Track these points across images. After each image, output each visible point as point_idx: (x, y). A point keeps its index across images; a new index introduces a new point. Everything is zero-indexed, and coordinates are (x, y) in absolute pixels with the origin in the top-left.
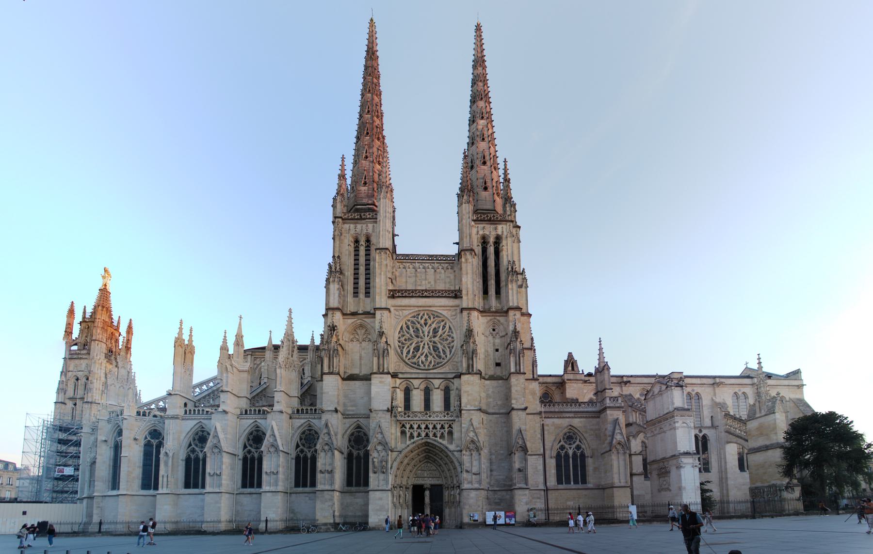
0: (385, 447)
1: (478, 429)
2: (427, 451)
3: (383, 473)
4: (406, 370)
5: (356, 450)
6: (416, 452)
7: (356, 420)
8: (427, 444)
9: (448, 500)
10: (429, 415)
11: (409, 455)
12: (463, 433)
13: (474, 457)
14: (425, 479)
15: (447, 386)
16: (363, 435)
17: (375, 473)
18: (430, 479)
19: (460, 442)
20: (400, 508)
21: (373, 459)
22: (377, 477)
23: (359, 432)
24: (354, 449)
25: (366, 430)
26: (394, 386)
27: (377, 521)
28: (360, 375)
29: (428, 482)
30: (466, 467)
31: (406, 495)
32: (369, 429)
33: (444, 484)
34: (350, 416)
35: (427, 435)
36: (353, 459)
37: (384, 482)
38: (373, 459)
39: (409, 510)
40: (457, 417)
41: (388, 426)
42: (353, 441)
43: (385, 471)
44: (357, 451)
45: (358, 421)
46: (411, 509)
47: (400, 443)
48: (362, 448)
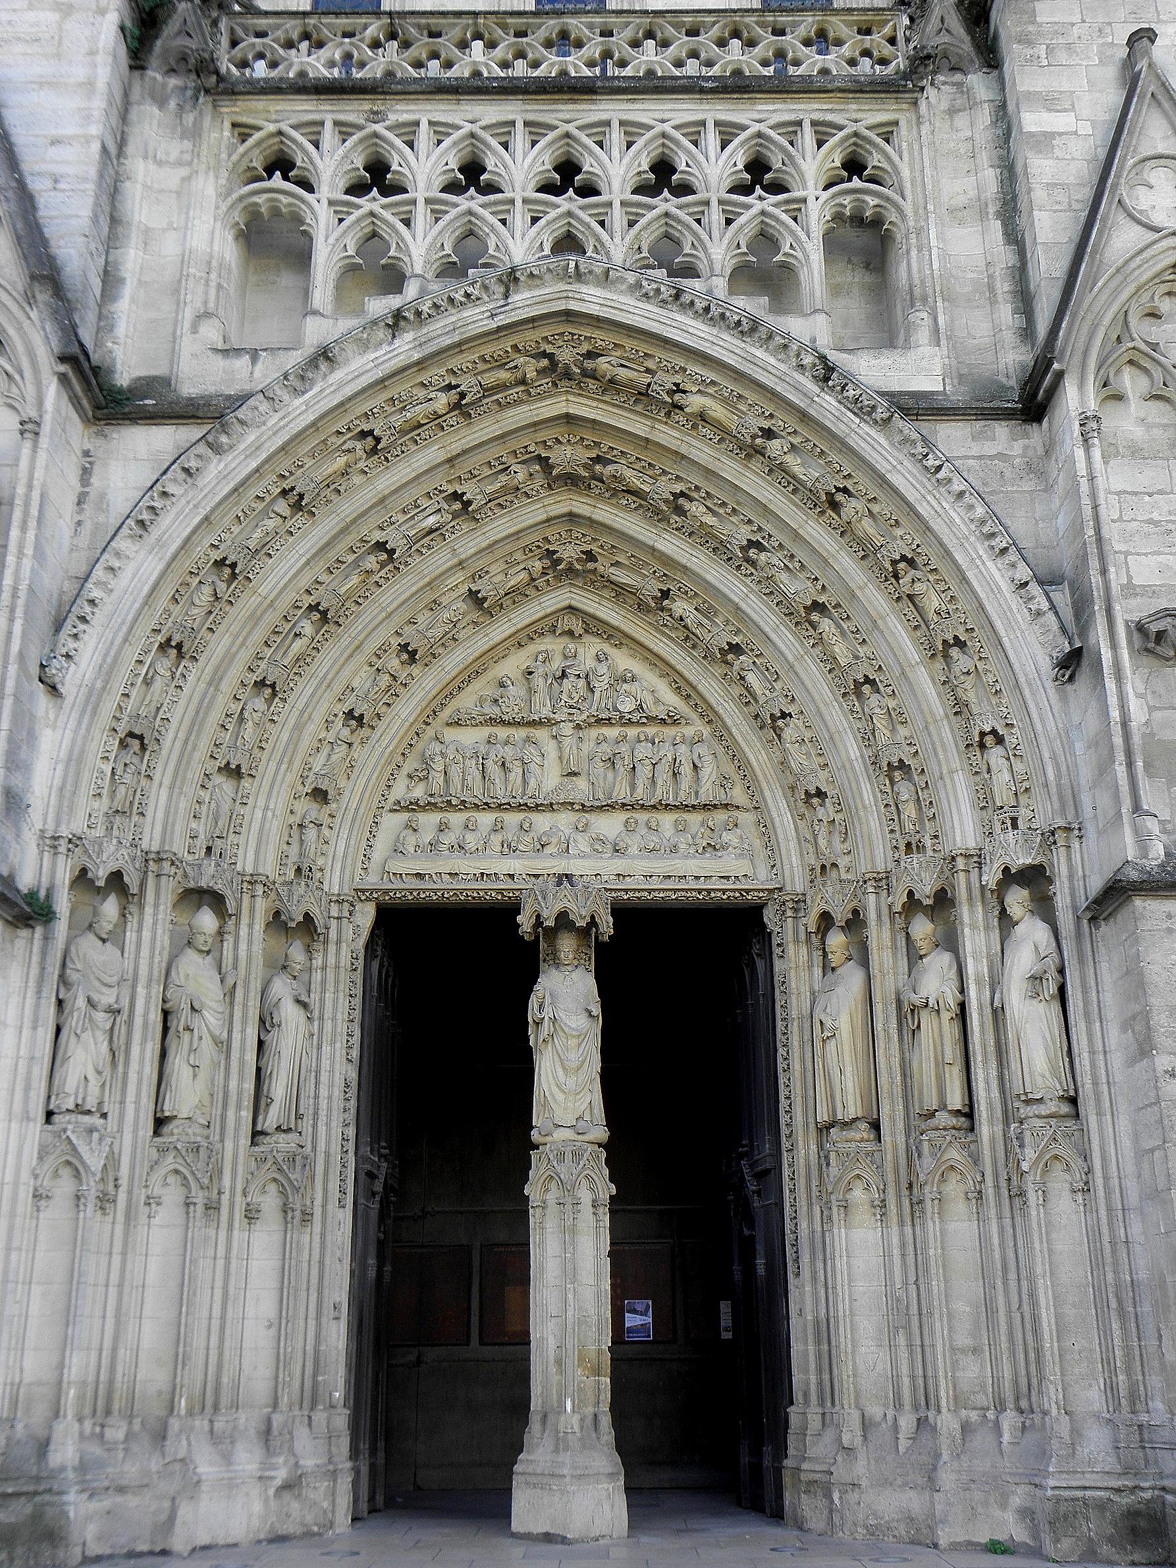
2: (567, 456)
6: (431, 454)
8: (566, 356)
9: (872, 1093)
10: (593, 49)
11: (335, 485)
14: (542, 822)
18: (610, 825)
19: (1006, 314)
20: (172, 1195)
29: (576, 867)
30: (1130, 589)
31: (266, 1022)
33: (796, 880)
35: (568, 243)
39: (309, 1239)
41: (70, 130)
46: (345, 1217)
47: (211, 333)
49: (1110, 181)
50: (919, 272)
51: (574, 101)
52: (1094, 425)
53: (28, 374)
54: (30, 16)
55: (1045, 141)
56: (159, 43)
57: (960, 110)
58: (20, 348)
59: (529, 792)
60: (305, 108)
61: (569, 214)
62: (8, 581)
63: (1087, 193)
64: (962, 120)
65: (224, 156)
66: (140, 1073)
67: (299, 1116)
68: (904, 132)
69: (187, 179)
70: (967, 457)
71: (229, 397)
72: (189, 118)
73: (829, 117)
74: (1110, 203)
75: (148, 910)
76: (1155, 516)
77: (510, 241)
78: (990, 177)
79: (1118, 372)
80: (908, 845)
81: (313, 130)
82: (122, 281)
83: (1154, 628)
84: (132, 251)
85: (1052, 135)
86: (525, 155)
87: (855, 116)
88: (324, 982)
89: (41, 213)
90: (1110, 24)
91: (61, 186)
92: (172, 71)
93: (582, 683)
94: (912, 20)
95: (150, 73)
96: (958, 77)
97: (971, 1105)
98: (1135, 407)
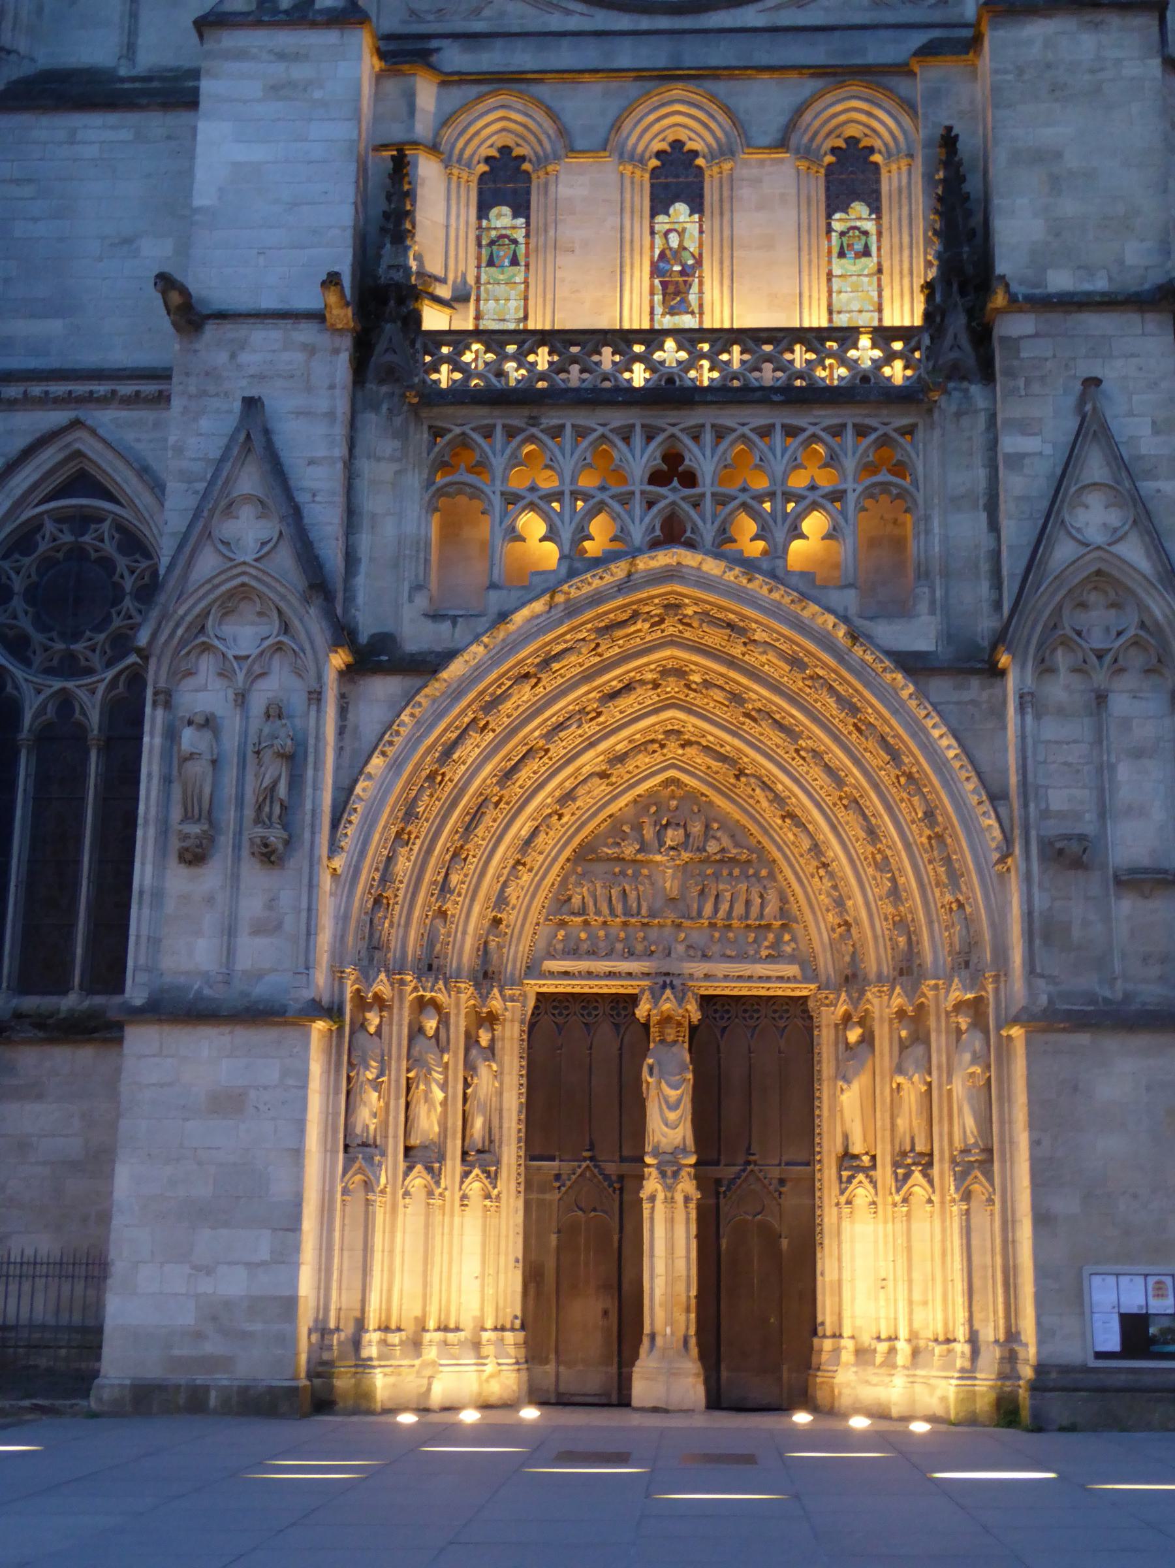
0: (286, 628)
1: (1151, 474)
3: (269, 856)
4: (502, 14)
5: (49, 671)
7: (59, 417)
12: (1006, 506)
13: (1126, 724)
15: (852, 141)
16: (109, 548)
17: (194, 856)
19: (984, 588)
21: (171, 735)
22: (210, 900)
23: (83, 521)
24: (27, 662)
25: (144, 498)
26: (396, 133)
27: (187, 1318)
28: (123, 72)
30: (1045, 814)
32: (158, 488)
34: (36, 390)
36: (17, 754)
37: (261, 942)
38: (171, 735)
40: (956, 373)
41: (321, 452)
42: (30, 595)
43: (275, 836)
44: (58, 684)
45: (76, 424)
47: (421, 602)
48: (96, 661)
49: (1056, 507)
50: (926, 551)
51: (679, 409)
52: (1028, 698)
53: (307, 646)
54: (286, 356)
55: (1017, 461)
56: (373, 359)
57: (966, 413)
58: (303, 636)
59: (644, 912)
60: (482, 415)
61: (673, 503)
62: (308, 806)
63: (1046, 504)
64: (965, 421)
65: (425, 455)
66: (396, 1118)
67: (491, 1142)
68: (920, 434)
69: (397, 473)
70: (948, 703)
71: (438, 654)
72: (398, 421)
73: (867, 421)
74: (1054, 526)
75: (395, 1011)
76: (1070, 759)
77: (631, 528)
78: (982, 473)
79: (1054, 650)
80: (901, 969)
81: (488, 433)
82: (359, 560)
83: (1058, 845)
84: (364, 536)
85: (1022, 456)
86: (643, 452)
87: (886, 420)
88: (503, 1048)
89: (306, 521)
90: (1074, 359)
91: (318, 499)
92: (382, 382)
93: (681, 831)
94: (932, 342)
95: (368, 386)
96: (965, 384)
97: (932, 1149)
98: (1064, 676)
